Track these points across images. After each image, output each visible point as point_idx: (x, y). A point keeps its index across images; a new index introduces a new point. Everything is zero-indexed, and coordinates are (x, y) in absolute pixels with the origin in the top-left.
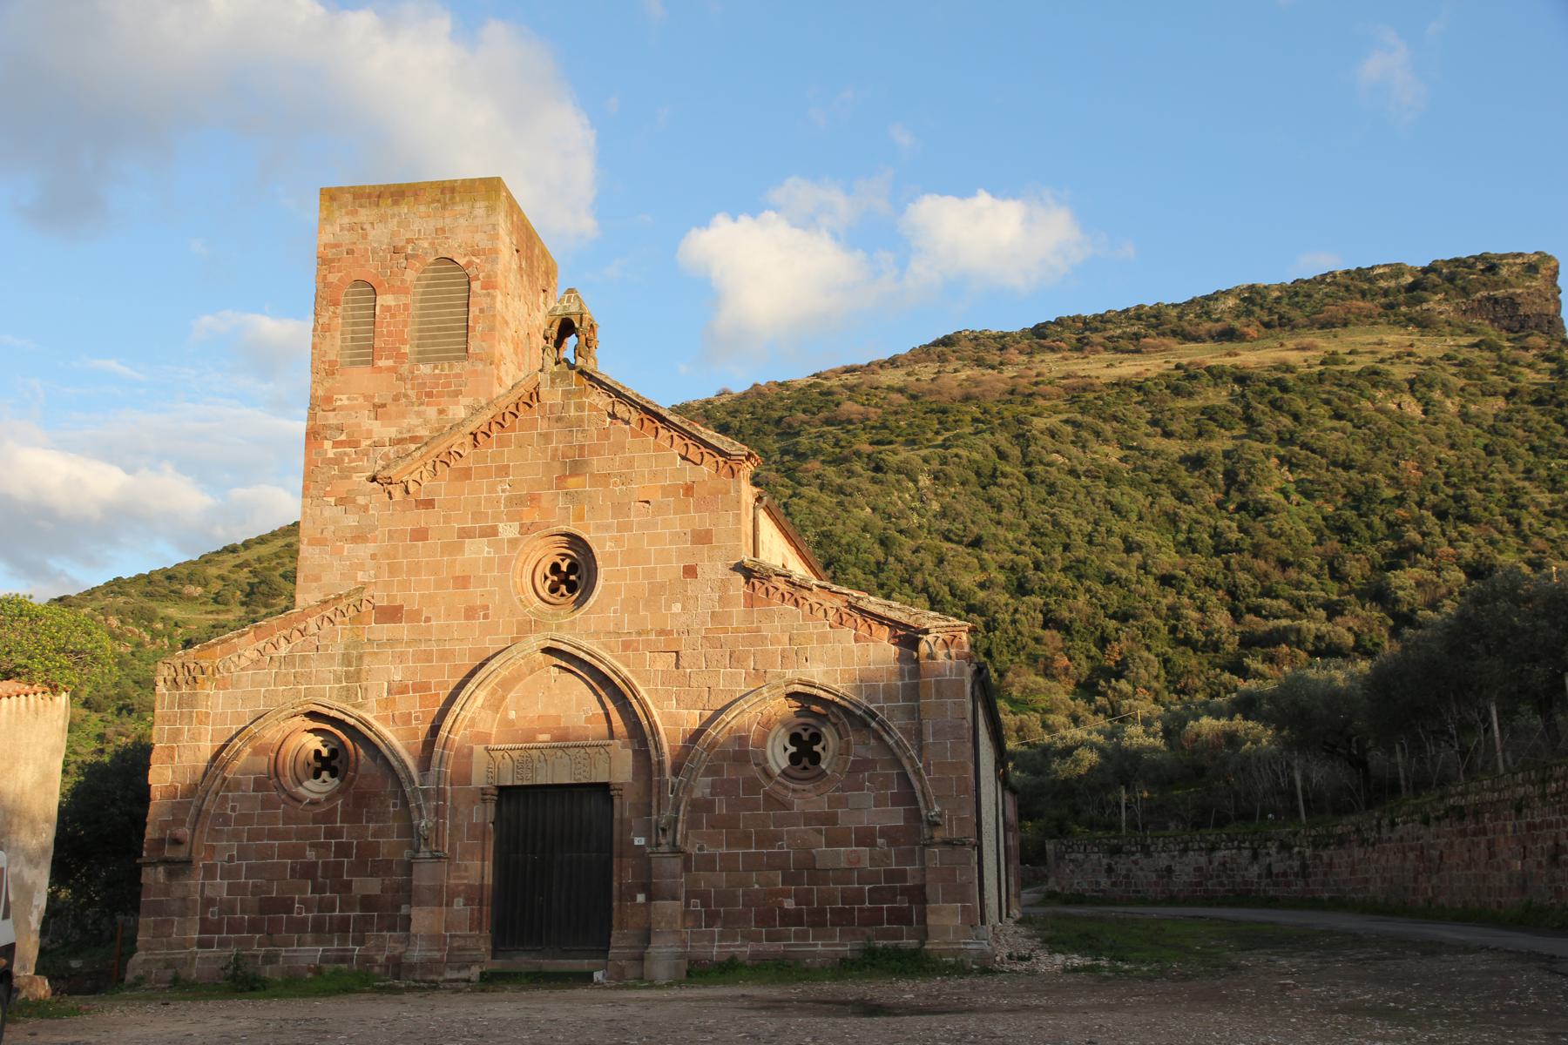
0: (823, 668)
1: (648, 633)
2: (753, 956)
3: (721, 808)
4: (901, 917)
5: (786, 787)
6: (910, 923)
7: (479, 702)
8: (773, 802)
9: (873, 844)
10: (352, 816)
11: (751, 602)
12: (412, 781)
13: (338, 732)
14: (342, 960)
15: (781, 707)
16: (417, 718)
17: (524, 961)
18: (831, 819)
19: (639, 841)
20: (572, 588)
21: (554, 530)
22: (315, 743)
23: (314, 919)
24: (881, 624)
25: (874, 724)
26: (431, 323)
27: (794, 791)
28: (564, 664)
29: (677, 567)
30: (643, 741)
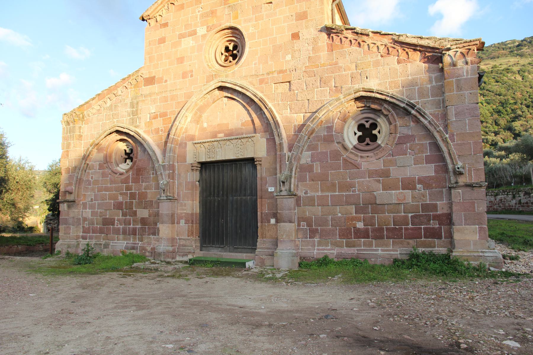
0: (377, 81)
1: (273, 73)
2: (338, 256)
3: (317, 169)
4: (434, 234)
5: (357, 156)
6: (440, 237)
7: (189, 119)
8: (349, 164)
9: (414, 188)
11: (331, 48)
12: (158, 161)
13: (129, 140)
14: (133, 248)
15: (353, 108)
16: (162, 130)
17: (215, 253)
18: (386, 174)
19: (271, 189)
20: (234, 57)
21: (223, 26)
22: (122, 146)
23: (123, 228)
24: (415, 50)
25: (413, 112)
27: (361, 157)
28: (229, 95)
29: (288, 35)
30: (272, 134)
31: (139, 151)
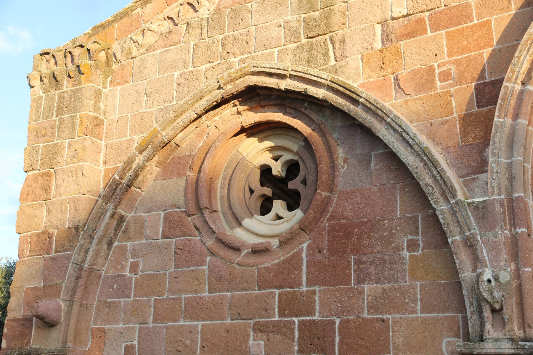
10: (330, 273)
12: (447, 191)
22: (257, 152)
31: (340, 162)
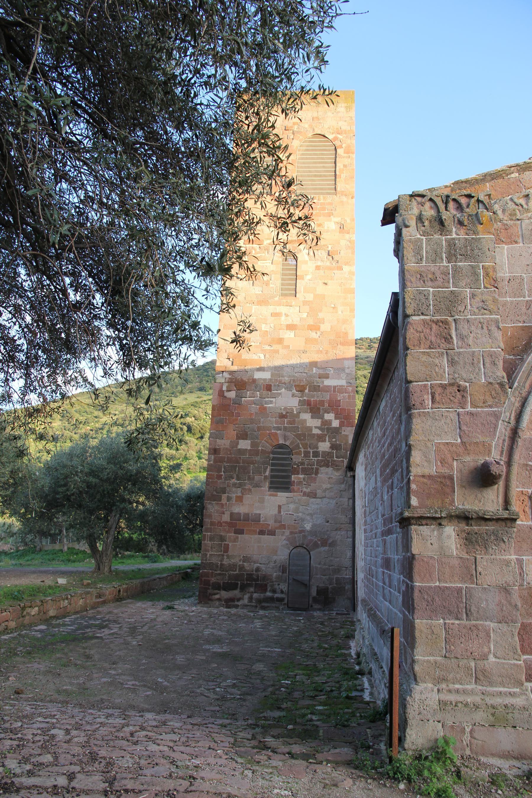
26: (310, 172)
